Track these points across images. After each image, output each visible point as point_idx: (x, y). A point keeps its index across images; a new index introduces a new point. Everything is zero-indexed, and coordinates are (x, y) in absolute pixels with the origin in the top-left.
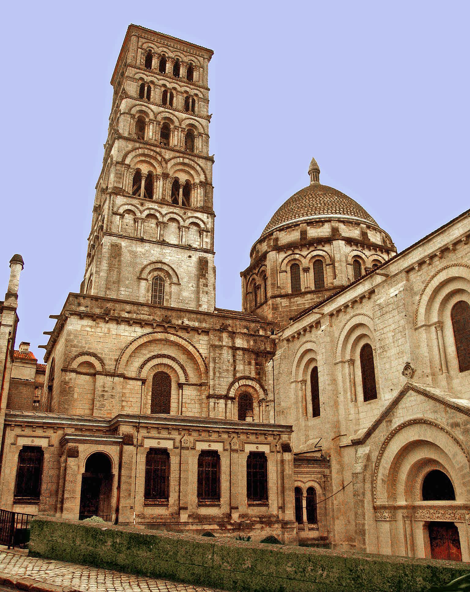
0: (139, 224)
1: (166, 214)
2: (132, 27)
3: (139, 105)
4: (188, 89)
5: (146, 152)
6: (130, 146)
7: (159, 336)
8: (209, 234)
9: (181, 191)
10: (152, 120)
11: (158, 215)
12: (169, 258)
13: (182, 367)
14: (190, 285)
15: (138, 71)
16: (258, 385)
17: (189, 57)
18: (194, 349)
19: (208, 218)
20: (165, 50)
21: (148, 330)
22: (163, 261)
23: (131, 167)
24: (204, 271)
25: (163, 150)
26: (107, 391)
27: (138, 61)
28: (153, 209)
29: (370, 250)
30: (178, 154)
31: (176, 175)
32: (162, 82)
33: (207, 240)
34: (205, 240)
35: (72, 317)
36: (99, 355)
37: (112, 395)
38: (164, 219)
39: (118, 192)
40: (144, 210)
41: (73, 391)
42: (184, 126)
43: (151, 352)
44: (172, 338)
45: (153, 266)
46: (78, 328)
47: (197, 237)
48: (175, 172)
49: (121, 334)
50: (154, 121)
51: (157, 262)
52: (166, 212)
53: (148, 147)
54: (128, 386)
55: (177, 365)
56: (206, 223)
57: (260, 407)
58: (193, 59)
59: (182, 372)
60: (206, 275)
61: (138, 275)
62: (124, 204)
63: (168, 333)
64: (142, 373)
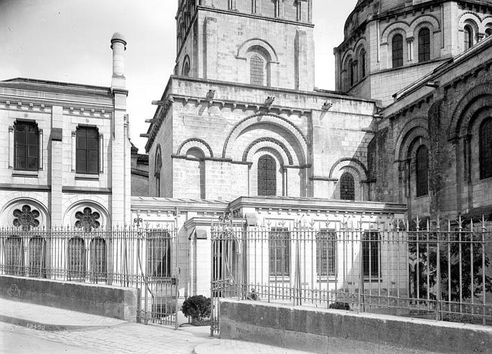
7: (265, 118)
21: (251, 113)
29: (484, 13)
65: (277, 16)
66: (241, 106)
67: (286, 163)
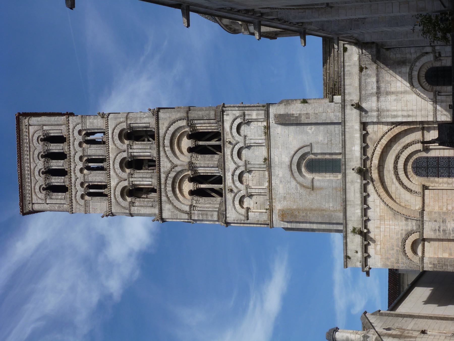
0: (253, 191)
1: (235, 163)
2: (24, 212)
3: (116, 199)
4: (77, 143)
5: (169, 188)
6: (166, 207)
8: (246, 112)
9: (201, 143)
10: (129, 183)
11: (238, 172)
12: (283, 156)
13: (406, 147)
14: (310, 131)
15: (74, 201)
16: (417, 64)
17: (35, 144)
18: (384, 138)
19: (228, 115)
20: (36, 173)
21: (370, 188)
22: (289, 163)
23: (190, 203)
24: (292, 118)
25: (162, 170)
26: (439, 227)
27: (63, 202)
28: (233, 178)
30: (162, 153)
31: (185, 150)
32: (79, 174)
33: (254, 115)
34: (254, 117)
35: (369, 264)
36: (404, 236)
37: (443, 222)
38: (240, 164)
39: (223, 214)
40: (236, 187)
41: (441, 258)
42: (125, 147)
43: (393, 183)
44: (375, 161)
45: (296, 174)
46: (378, 257)
47: (253, 125)
48: (182, 153)
49: (379, 214)
50: (129, 181)
51: (292, 171)
52: (232, 163)
53: (163, 187)
54: (432, 204)
55: (403, 153)
56: (234, 117)
57: (441, 60)
58: (35, 138)
59: (410, 147)
60: (295, 115)
61: (308, 190)
62: (235, 208)
63: (371, 166)
64: (416, 190)
65: (264, 144)
66: (365, 200)
67: (419, 146)
